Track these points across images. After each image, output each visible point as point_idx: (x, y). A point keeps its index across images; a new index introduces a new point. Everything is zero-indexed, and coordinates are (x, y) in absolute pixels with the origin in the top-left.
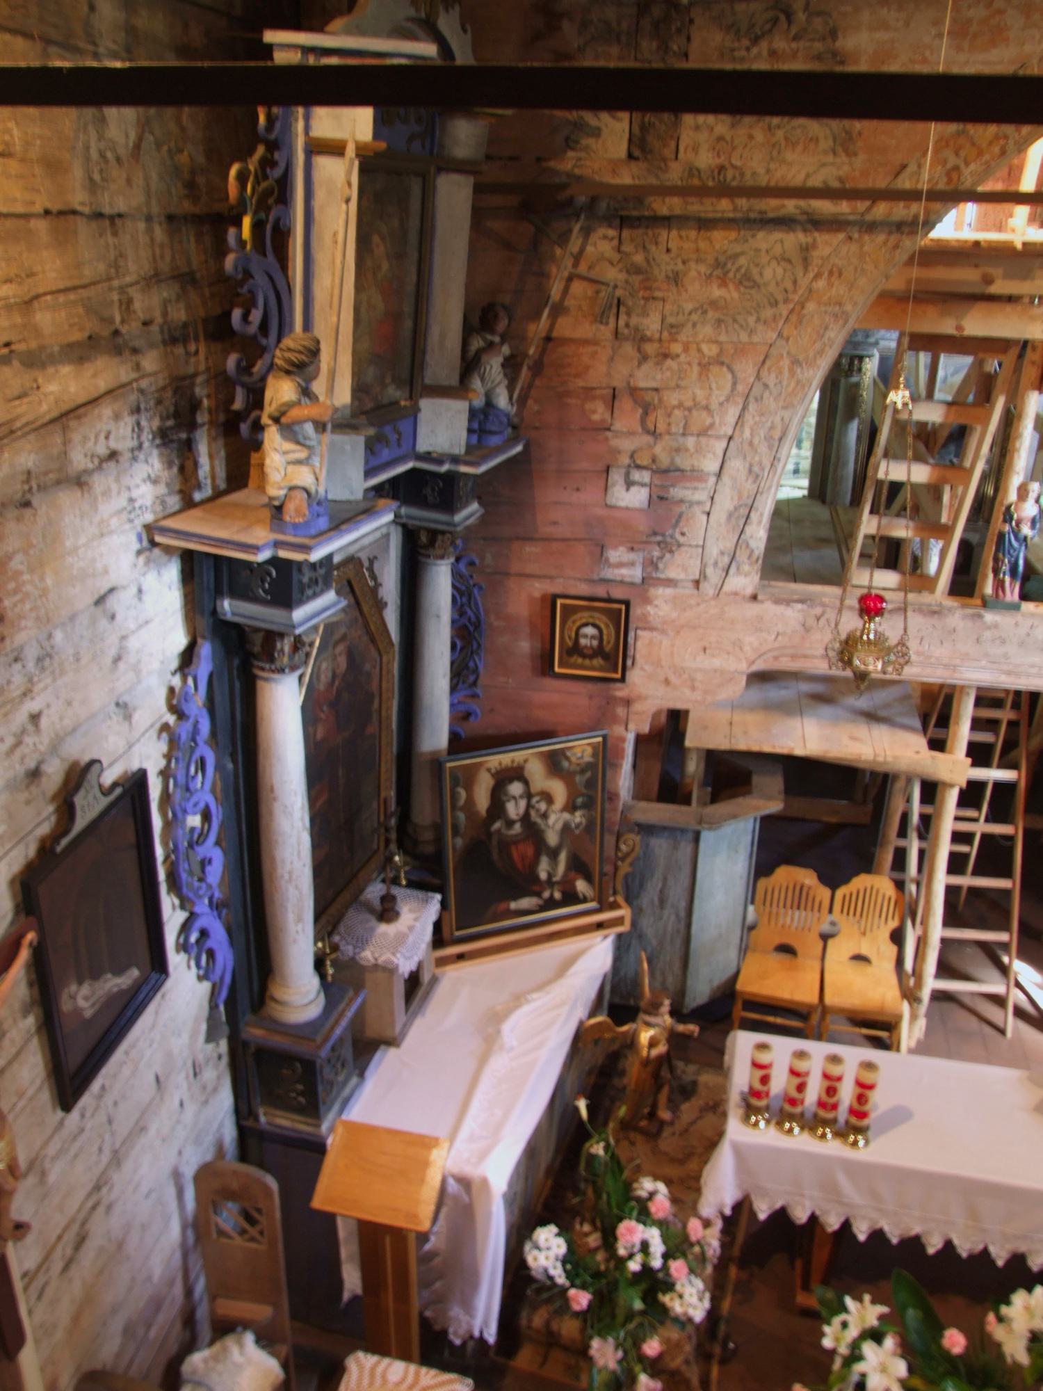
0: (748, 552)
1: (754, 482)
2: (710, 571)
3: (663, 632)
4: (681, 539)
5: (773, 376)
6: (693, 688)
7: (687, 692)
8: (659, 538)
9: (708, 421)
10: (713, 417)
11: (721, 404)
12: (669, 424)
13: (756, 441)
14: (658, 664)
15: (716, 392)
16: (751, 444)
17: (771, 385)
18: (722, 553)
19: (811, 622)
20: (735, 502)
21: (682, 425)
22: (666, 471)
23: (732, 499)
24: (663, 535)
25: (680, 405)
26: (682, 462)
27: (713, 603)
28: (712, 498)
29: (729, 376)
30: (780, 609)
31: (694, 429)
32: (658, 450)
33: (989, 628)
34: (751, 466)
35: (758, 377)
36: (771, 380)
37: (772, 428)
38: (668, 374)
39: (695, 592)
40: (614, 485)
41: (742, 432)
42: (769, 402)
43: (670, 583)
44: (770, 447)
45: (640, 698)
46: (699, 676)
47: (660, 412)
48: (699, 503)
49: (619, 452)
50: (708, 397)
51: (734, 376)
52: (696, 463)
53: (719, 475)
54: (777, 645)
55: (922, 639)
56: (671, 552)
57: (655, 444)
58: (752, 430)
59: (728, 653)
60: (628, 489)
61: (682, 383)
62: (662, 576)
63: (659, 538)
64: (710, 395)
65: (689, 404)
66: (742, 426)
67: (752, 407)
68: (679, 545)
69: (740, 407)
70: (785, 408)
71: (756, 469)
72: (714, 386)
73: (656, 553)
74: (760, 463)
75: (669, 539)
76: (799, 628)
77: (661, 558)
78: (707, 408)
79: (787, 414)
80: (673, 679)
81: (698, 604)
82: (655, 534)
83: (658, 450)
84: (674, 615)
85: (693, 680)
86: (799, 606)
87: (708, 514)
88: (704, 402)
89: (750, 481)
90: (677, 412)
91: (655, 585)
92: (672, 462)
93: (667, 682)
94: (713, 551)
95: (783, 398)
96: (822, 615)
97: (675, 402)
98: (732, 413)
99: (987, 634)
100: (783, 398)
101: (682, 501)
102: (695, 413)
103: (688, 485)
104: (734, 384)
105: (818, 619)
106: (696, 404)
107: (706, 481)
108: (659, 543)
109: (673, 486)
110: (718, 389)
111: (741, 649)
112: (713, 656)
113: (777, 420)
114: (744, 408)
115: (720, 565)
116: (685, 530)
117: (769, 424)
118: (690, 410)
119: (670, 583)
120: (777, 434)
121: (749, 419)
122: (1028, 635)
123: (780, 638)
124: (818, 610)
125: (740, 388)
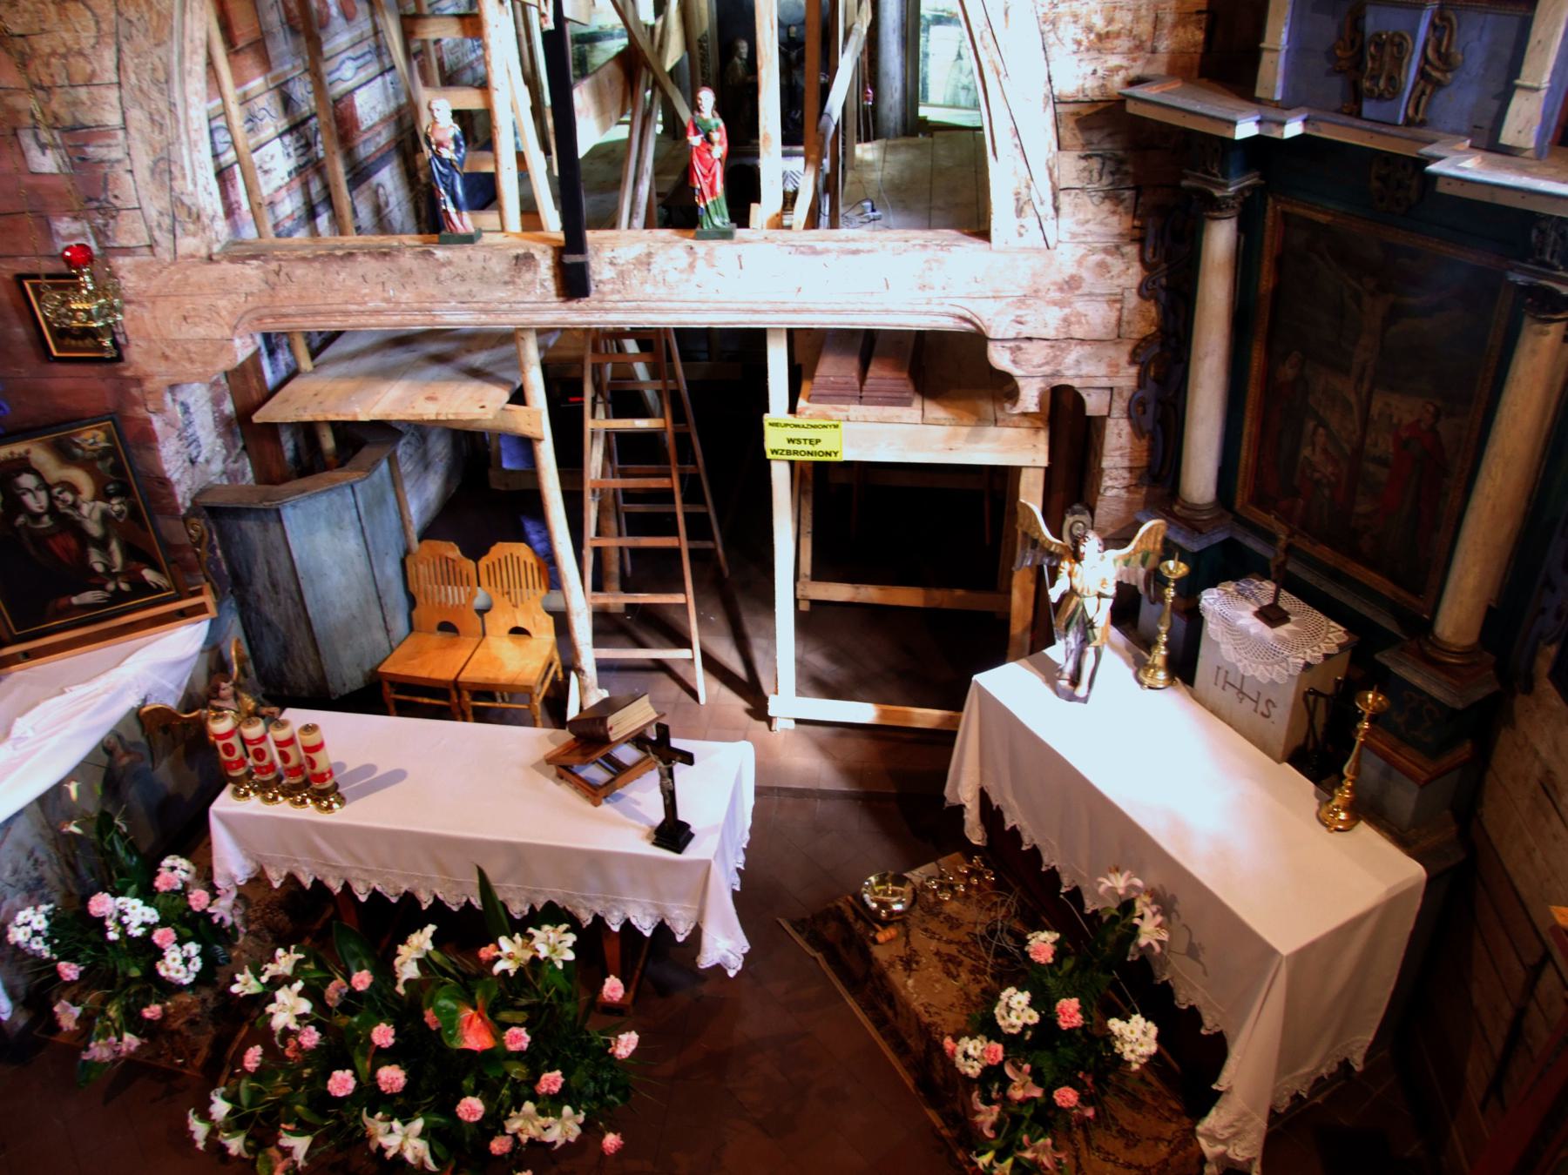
0: (186, 210)
1: (161, 133)
2: (157, 234)
3: (141, 304)
4: (118, 203)
5: (132, 9)
6: (192, 361)
7: (188, 365)
8: (96, 204)
9: (89, 69)
10: (90, 63)
11: (93, 47)
12: (52, 76)
13: (145, 87)
14: (148, 338)
15: (84, 34)
16: (141, 90)
17: (134, 19)
18: (161, 214)
19: (273, 278)
20: (152, 158)
21: (64, 75)
22: (73, 129)
23: (147, 154)
24: (97, 200)
25: (54, 53)
26: (88, 119)
27: (173, 268)
28: (129, 154)
29: (89, 14)
30: (237, 268)
31: (79, 79)
32: (55, 105)
33: (443, 265)
34: (151, 114)
35: (119, 14)
36: (131, 13)
37: (154, 70)
38: (27, 16)
39: (153, 258)
40: (28, 150)
41: (128, 78)
42: (139, 39)
43: (127, 251)
44: (161, 91)
45: (148, 376)
46: (192, 348)
47: (37, 62)
48: (119, 161)
49: (19, 112)
50: (78, 40)
51: (94, 15)
52: (98, 118)
53: (125, 128)
54: (249, 306)
55: (383, 283)
56: (113, 217)
57: (50, 100)
58: (136, 73)
59: (208, 320)
60: (44, 154)
61: (46, 27)
62: (116, 245)
63: (96, 204)
64: (78, 38)
65: (62, 50)
66: (126, 71)
67: (126, 47)
68: (118, 210)
69: (114, 48)
70: (158, 45)
71: (157, 117)
72: (78, 27)
73: (100, 221)
74: (158, 111)
75: (106, 205)
76: (264, 286)
77: (106, 225)
78: (81, 53)
79: (160, 51)
80: (168, 352)
81: (160, 272)
82: (90, 200)
83: (55, 105)
84: (143, 285)
85: (188, 352)
86: (255, 263)
87: (131, 171)
88: (76, 47)
89: (157, 133)
90: (53, 60)
91: (114, 256)
92: (74, 118)
93: (166, 357)
94: (152, 212)
95: (151, 34)
96: (280, 270)
97: (48, 50)
98: (109, 57)
99: (444, 271)
100: (151, 34)
101: (102, 161)
102: (71, 60)
103: (100, 143)
104: (97, 22)
105: (277, 273)
106: (69, 50)
107: (114, 136)
108: (97, 209)
109: (87, 145)
110: (84, 30)
111: (218, 314)
112: (196, 325)
113: (157, 61)
114: (119, 50)
115: (164, 227)
116: (116, 192)
117: (149, 66)
118: (64, 56)
119: (127, 251)
120: (161, 76)
121: (130, 62)
122: (484, 268)
123: (250, 298)
124: (274, 265)
125: (104, 26)
